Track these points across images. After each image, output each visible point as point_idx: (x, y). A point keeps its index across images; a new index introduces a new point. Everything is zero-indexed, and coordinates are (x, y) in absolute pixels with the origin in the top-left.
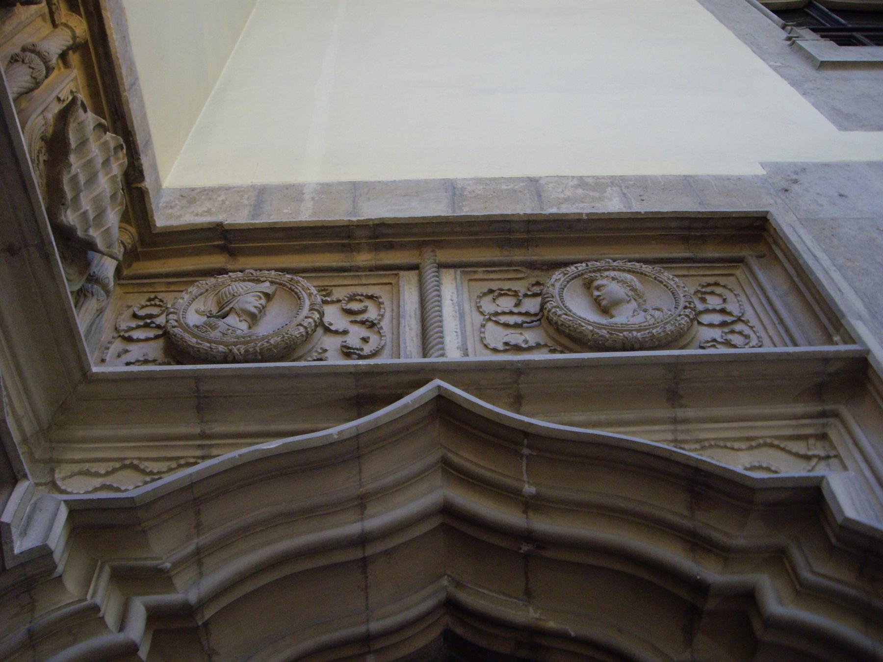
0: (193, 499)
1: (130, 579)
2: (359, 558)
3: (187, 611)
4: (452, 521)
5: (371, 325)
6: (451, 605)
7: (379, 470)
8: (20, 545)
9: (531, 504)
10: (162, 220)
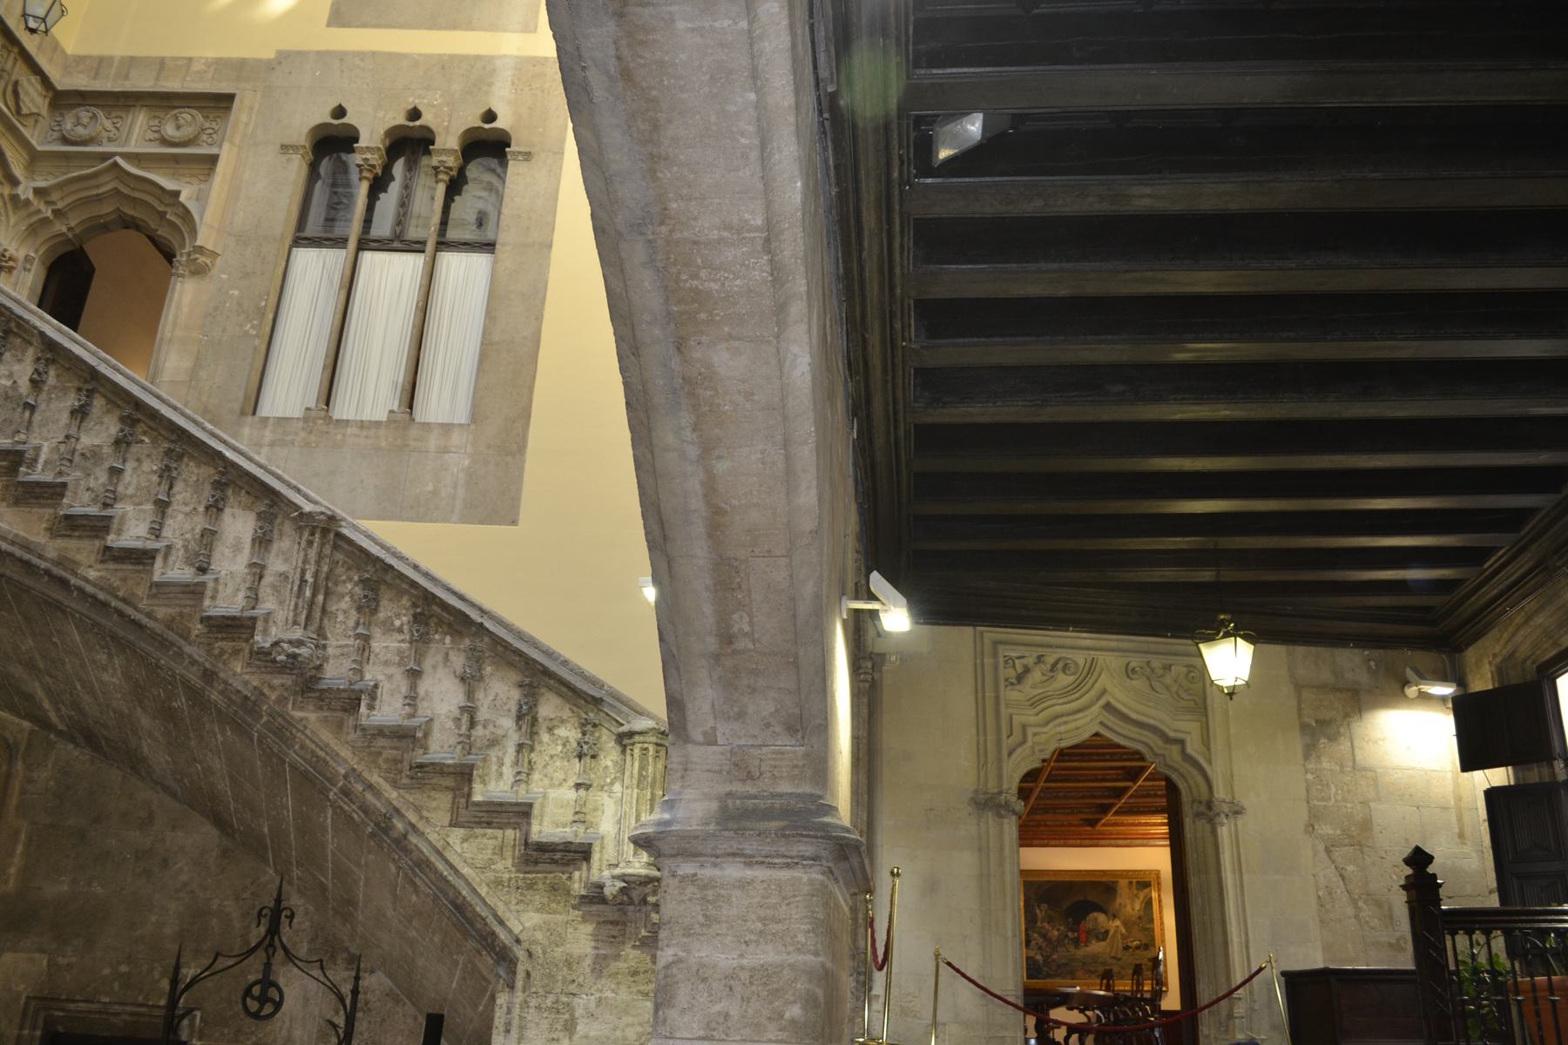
0: (60, 186)
1: (48, 203)
2: (98, 199)
4: (117, 192)
7: (102, 179)
10: (62, 82)
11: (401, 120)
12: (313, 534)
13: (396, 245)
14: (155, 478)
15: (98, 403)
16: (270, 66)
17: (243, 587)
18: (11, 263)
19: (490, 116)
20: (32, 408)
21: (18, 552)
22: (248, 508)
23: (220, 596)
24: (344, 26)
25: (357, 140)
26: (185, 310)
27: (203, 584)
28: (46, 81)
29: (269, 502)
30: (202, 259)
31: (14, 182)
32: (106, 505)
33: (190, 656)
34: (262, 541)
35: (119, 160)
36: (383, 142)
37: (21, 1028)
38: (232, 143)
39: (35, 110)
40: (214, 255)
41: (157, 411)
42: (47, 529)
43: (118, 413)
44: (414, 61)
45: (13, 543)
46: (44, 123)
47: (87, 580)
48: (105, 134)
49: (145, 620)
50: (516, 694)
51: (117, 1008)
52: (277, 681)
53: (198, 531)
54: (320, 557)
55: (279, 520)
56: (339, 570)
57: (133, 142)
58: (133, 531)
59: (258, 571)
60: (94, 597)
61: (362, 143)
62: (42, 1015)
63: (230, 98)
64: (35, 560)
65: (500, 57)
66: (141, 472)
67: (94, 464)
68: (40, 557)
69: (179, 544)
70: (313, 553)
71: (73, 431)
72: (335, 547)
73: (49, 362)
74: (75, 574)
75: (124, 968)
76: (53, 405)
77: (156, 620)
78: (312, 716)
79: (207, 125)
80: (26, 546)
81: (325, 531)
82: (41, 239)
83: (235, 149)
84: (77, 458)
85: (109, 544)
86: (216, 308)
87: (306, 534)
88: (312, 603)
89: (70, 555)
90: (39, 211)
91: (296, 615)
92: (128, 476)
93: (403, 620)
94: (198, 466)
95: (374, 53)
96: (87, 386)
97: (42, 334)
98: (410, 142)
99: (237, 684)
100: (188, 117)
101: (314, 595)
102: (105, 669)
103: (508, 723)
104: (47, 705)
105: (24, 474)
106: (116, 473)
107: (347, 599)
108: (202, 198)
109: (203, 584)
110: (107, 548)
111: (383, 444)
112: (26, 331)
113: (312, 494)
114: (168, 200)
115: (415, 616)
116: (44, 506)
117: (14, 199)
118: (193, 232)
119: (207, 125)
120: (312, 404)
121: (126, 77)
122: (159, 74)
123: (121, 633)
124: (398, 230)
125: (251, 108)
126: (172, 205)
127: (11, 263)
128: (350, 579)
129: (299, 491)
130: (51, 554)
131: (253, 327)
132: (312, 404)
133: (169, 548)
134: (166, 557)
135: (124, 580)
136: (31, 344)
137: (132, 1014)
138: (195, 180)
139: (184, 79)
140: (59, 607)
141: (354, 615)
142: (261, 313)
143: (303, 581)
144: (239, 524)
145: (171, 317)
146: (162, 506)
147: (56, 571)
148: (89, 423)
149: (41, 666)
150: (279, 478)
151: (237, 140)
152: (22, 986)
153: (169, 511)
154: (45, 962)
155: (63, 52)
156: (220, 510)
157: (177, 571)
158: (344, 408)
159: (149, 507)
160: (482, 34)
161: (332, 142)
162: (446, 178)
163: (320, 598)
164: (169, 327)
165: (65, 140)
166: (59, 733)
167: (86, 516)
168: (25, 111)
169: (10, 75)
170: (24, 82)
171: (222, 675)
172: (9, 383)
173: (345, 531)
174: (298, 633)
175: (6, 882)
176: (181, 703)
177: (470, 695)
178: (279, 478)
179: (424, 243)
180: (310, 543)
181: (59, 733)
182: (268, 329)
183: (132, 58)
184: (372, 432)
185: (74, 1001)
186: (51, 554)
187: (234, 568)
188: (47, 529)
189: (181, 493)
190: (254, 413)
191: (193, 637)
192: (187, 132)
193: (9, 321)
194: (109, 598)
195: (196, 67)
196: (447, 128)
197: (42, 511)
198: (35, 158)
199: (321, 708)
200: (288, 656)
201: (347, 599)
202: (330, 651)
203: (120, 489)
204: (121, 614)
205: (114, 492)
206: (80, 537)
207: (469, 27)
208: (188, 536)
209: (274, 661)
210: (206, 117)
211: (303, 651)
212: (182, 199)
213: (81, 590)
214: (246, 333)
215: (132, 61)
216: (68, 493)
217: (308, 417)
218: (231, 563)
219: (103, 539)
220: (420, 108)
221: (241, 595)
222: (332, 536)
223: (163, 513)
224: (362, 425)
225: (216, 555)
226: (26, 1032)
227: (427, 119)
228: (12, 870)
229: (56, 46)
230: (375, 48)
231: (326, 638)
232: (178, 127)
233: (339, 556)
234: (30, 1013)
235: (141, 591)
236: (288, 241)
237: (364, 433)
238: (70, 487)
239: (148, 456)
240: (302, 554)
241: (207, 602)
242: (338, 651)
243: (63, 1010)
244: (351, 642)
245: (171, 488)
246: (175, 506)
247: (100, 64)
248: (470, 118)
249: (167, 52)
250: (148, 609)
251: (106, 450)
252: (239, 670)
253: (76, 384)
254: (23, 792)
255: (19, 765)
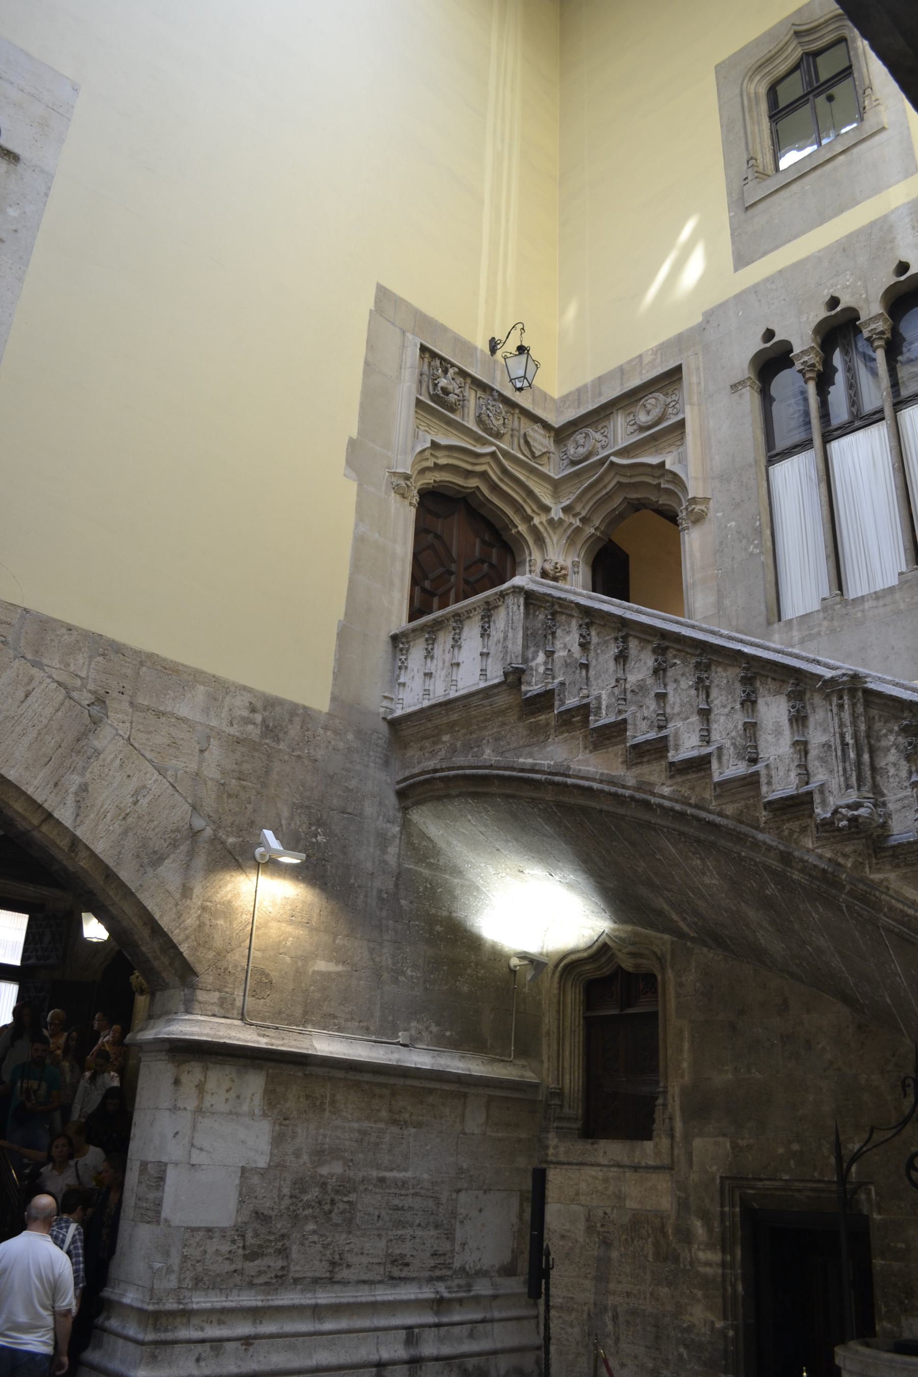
0: (579, 498)
1: (575, 516)
2: (609, 496)
3: (584, 517)
4: (620, 484)
5: (606, 436)
6: (625, 498)
7: (606, 480)
8: (556, 519)
9: (630, 477)
10: (557, 421)
11: (823, 314)
12: (841, 698)
13: (857, 424)
14: (693, 692)
15: (633, 644)
16: (701, 329)
17: (793, 766)
18: (563, 572)
19: (903, 267)
20: (586, 667)
21: (606, 788)
22: (778, 693)
23: (775, 780)
24: (748, 264)
25: (792, 351)
26: (697, 555)
27: (757, 774)
28: (546, 426)
29: (797, 683)
30: (697, 508)
31: (546, 509)
32: (661, 728)
33: (764, 843)
34: (799, 719)
35: (613, 458)
36: (814, 340)
37: (722, 1206)
38: (691, 404)
39: (544, 450)
40: (706, 500)
41: (678, 634)
42: (623, 763)
43: (650, 647)
44: (816, 259)
45: (601, 782)
46: (555, 457)
47: (663, 797)
48: (599, 445)
49: (718, 820)
51: (800, 1185)
52: (848, 849)
53: (740, 727)
54: (854, 717)
55: (808, 695)
56: (878, 725)
57: (620, 441)
58: (688, 744)
59: (802, 747)
60: (672, 809)
61: (797, 350)
62: (737, 1193)
63: (678, 369)
64: (621, 791)
65: (893, 212)
66: (681, 689)
67: (644, 696)
68: (624, 787)
69: (728, 743)
70: (846, 716)
71: (620, 674)
72: (867, 705)
73: (589, 625)
74: (653, 794)
75: (795, 1147)
76: (601, 659)
77: (727, 817)
78: (892, 876)
79: (669, 400)
80: (611, 782)
81: (852, 691)
82: (579, 545)
83: (696, 408)
84: (629, 696)
85: (671, 759)
86: (721, 544)
87: (835, 700)
88: (859, 763)
89: (647, 778)
90: (571, 524)
91: (847, 779)
92: (671, 698)
94: (725, 670)
95: (780, 272)
96: (620, 634)
97: (578, 605)
98: (840, 329)
99: (812, 859)
100: (653, 401)
101: (859, 755)
102: (704, 874)
104: (674, 917)
105: (595, 722)
106: (661, 697)
107: (893, 751)
108: (682, 460)
109: (757, 774)
110: (672, 764)
111: (902, 606)
112: (567, 608)
113: (832, 662)
114: (657, 473)
116: (615, 744)
117: (551, 522)
118: (684, 488)
119: (669, 400)
120: (826, 594)
121: (600, 394)
122: (622, 380)
123: (702, 836)
124: (854, 410)
125: (698, 369)
126: (662, 475)
127: (563, 572)
128: (891, 731)
129: (818, 663)
130: (631, 782)
131: (756, 547)
132: (826, 594)
133: (720, 749)
134: (720, 758)
135: (692, 788)
136: (573, 616)
137: (813, 1190)
138: (673, 448)
139: (641, 373)
140: (649, 826)
141: (904, 765)
142: (759, 532)
143: (844, 745)
144: (774, 710)
145: (688, 566)
146: (705, 714)
147: (639, 795)
148: (631, 664)
149: (658, 883)
150: (797, 657)
151: (695, 399)
152: (715, 1168)
153: (712, 717)
154: (728, 1144)
155: (552, 398)
156: (754, 703)
157: (731, 768)
158: (856, 587)
159: (695, 718)
160: (869, 201)
161: (772, 361)
162: (881, 343)
163: (866, 757)
164: (689, 574)
165: (573, 463)
166: (692, 939)
167: (647, 742)
168: (537, 453)
169: (519, 431)
170: (531, 432)
171: (796, 854)
172: (565, 653)
173: (871, 686)
174: (853, 796)
175: (683, 1076)
176: (771, 889)
178: (797, 657)
179: (881, 410)
180: (841, 707)
181: (692, 939)
182: (769, 544)
183: (599, 378)
184: (888, 599)
185: (761, 1180)
186: (631, 782)
187: (781, 751)
188: (623, 763)
189: (719, 698)
190: (780, 620)
191: (762, 825)
192: (656, 413)
193: (553, 605)
194: (685, 808)
195: (646, 360)
196: (867, 300)
197: (616, 748)
198: (556, 486)
199: (898, 866)
200: (849, 820)
201: (893, 751)
202: (891, 806)
203: (668, 710)
205: (664, 715)
206: (649, 762)
207: (855, 202)
208: (734, 734)
209: (840, 830)
210: (666, 395)
211: (862, 811)
212: (667, 467)
213: (660, 806)
214: (751, 554)
215: (600, 380)
216: (629, 727)
217: (826, 606)
218: (777, 747)
219: (667, 757)
220: (837, 295)
221: (793, 774)
222: (860, 694)
223: (708, 720)
224: (877, 596)
225: (762, 744)
226: (727, 1209)
227: (846, 301)
228: (685, 1065)
229: (545, 396)
230: (779, 268)
231: (883, 795)
232: (648, 413)
233: (874, 712)
234: (727, 1191)
235: (708, 795)
236: (763, 462)
237: (881, 603)
238: (630, 721)
239: (683, 675)
240: (836, 719)
241: (764, 789)
242: (899, 805)
243: (753, 1188)
244: (908, 792)
245: (708, 696)
246: (716, 711)
247: (580, 392)
248: (886, 278)
249: (622, 360)
250: (718, 809)
251: (650, 681)
252: (810, 846)
253: (613, 635)
254: (678, 995)
255: (670, 973)
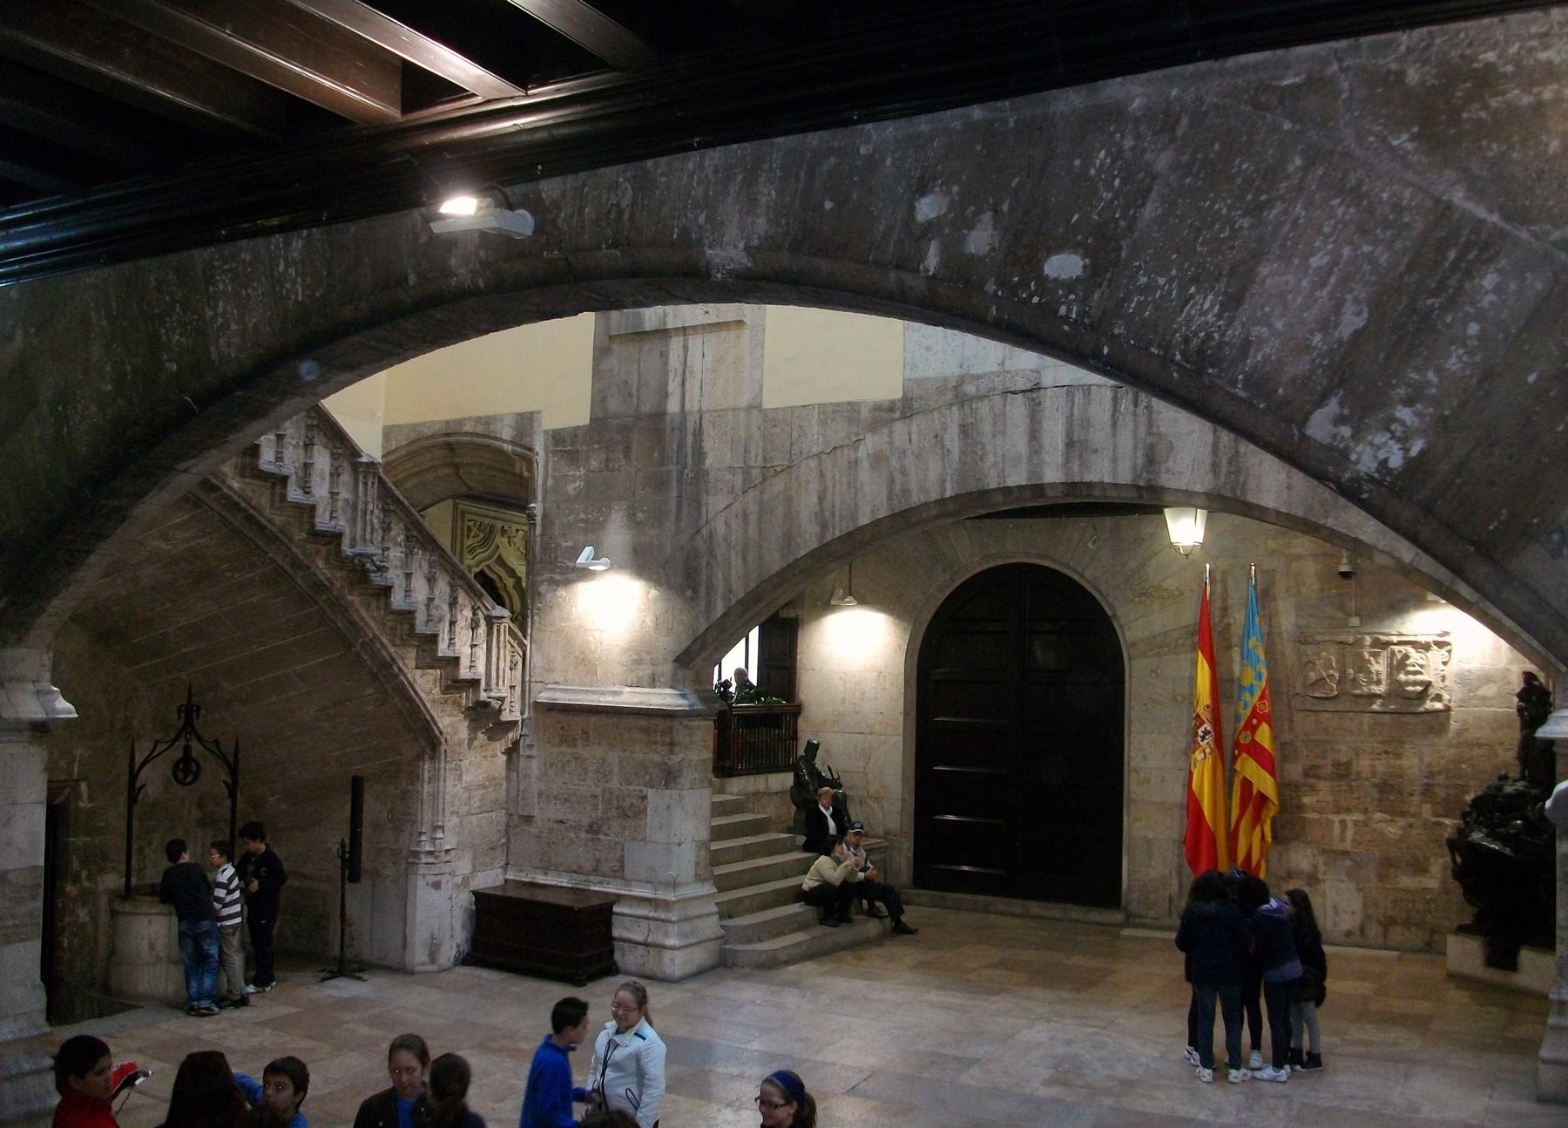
34: (335, 475)
47: (230, 488)
50: (448, 589)
59: (333, 495)
60: (237, 504)
74: (223, 482)
93: (401, 538)
103: (446, 607)
115: (407, 537)
144: (322, 460)
177: (431, 588)
204: (250, 518)
213: (228, 498)
